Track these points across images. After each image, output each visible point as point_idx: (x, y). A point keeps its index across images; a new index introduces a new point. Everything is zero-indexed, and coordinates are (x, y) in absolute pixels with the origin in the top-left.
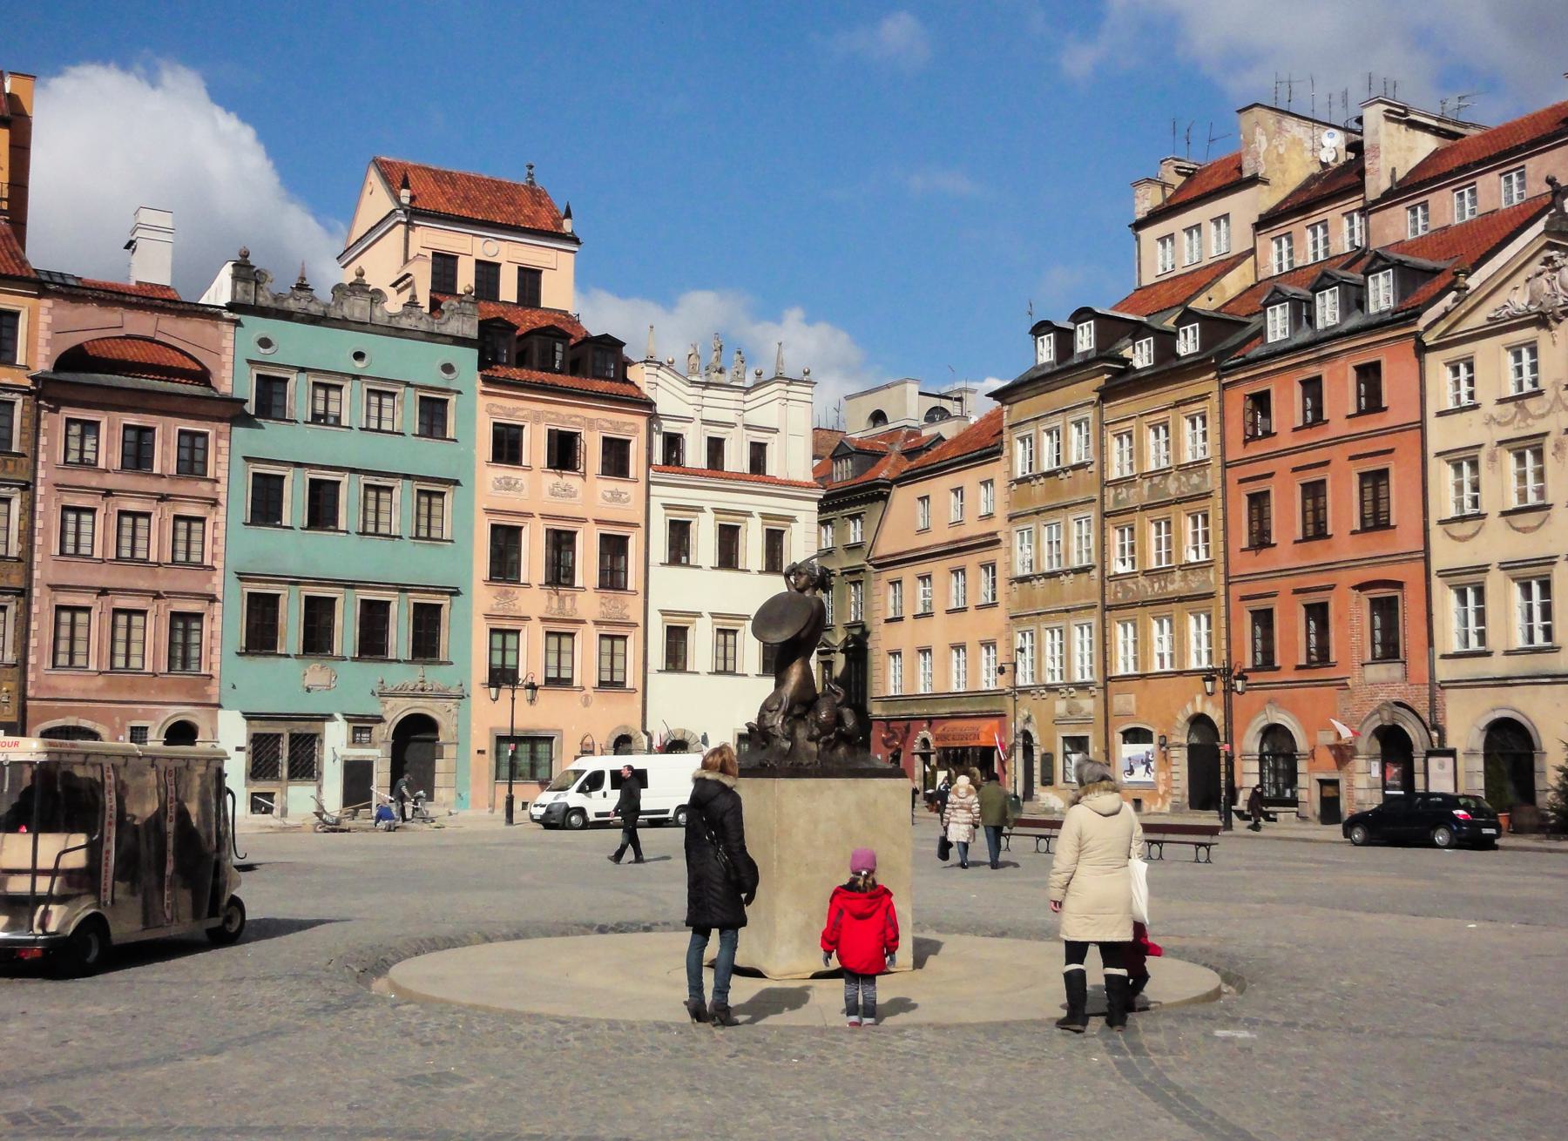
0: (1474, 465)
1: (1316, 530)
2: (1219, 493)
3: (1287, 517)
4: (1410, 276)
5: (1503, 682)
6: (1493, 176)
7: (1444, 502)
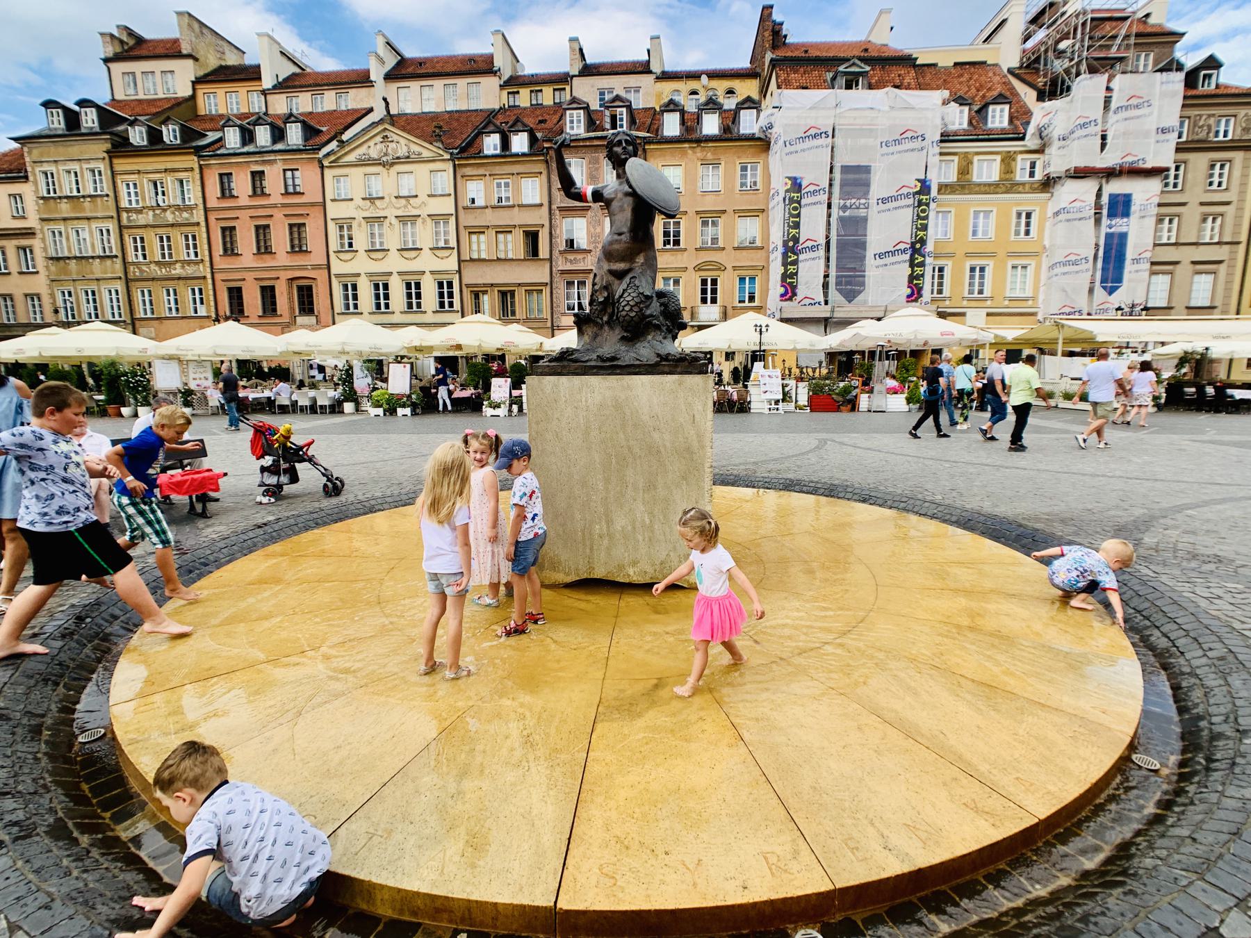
0: (350, 228)
1: (264, 248)
2: (203, 224)
3: (246, 240)
4: (310, 131)
7: (334, 245)
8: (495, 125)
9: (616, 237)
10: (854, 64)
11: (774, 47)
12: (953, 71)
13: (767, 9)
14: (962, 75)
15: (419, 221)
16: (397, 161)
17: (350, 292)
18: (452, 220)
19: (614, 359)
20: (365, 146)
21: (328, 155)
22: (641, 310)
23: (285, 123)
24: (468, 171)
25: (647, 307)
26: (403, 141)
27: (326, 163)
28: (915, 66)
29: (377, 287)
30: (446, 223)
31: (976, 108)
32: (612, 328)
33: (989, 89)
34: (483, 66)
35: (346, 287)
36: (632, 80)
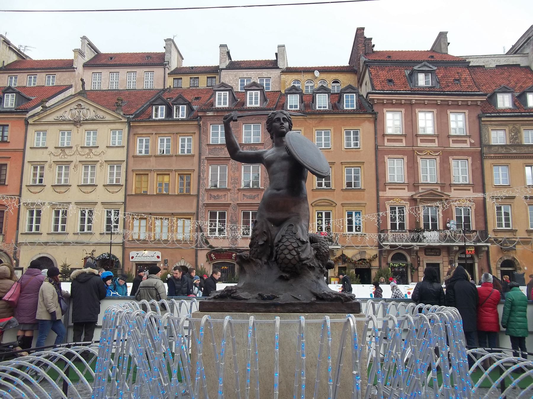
0: (42, 168)
5: (46, 244)
6: (44, 75)
8: (162, 99)
9: (275, 192)
10: (425, 65)
11: (366, 54)
12: (496, 70)
13: (360, 31)
14: (502, 73)
15: (98, 165)
16: (87, 121)
17: (35, 217)
18: (124, 164)
19: (273, 297)
20: (63, 111)
21: (34, 116)
22: (298, 253)
23: (4, 93)
24: (140, 131)
25: (303, 251)
26: (92, 109)
27: (31, 121)
28: (469, 67)
29: (57, 213)
30: (119, 167)
31: (517, 94)
32: (270, 268)
33: (525, 83)
34: (157, 61)
35: (32, 213)
36: (265, 73)
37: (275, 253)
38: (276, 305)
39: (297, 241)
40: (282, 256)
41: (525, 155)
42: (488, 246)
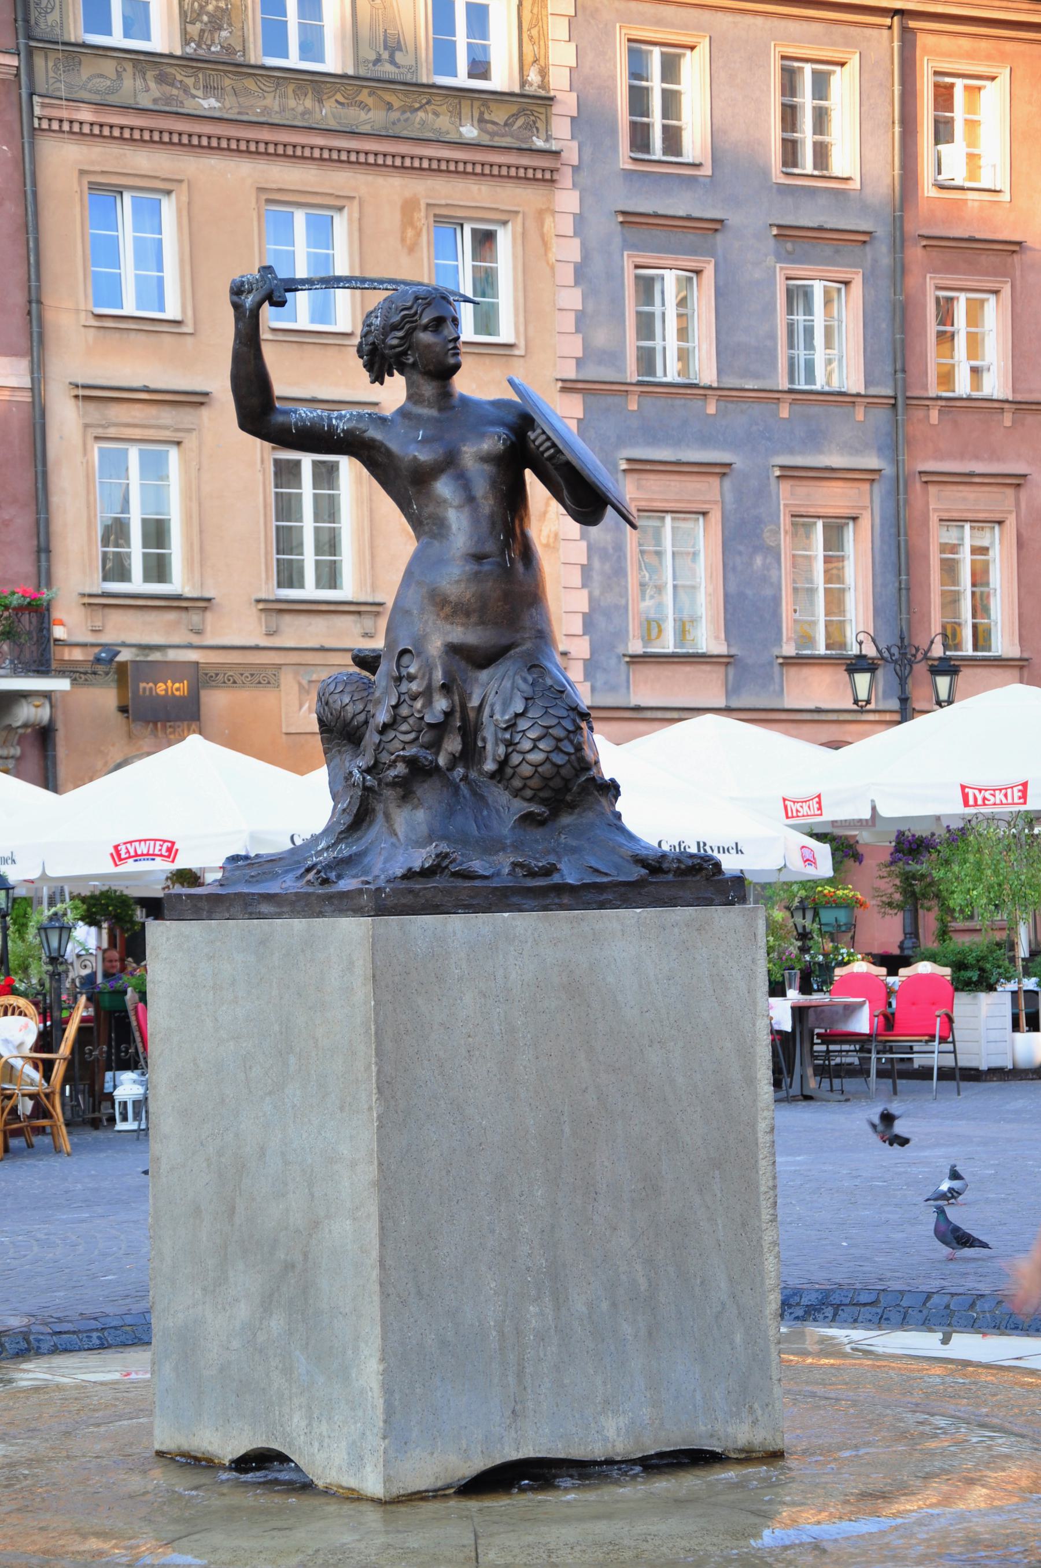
19: (549, 871)
22: (579, 748)
37: (493, 751)
38: (561, 889)
39: (571, 713)
40: (536, 757)
41: (265, 135)
42: (47, 695)
